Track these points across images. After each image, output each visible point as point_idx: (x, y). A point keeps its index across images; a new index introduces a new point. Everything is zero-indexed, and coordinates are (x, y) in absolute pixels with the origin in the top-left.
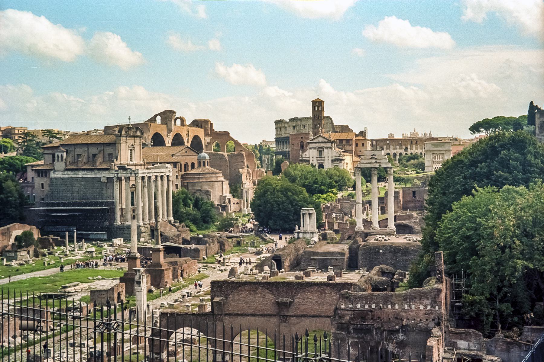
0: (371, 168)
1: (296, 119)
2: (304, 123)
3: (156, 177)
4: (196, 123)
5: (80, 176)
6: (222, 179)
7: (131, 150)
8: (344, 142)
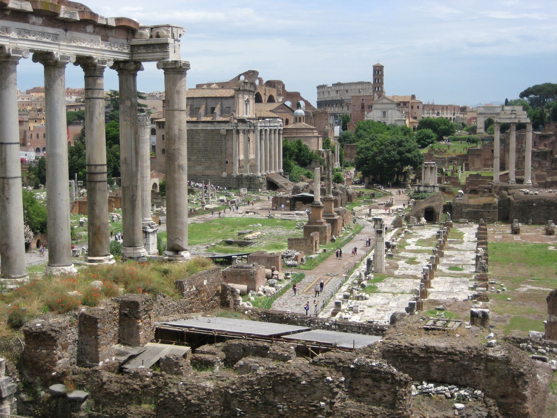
0: (510, 123)
1: (339, 84)
2: (346, 88)
3: (271, 130)
4: (270, 84)
5: (200, 128)
6: (317, 134)
7: (246, 104)
8: (402, 105)
